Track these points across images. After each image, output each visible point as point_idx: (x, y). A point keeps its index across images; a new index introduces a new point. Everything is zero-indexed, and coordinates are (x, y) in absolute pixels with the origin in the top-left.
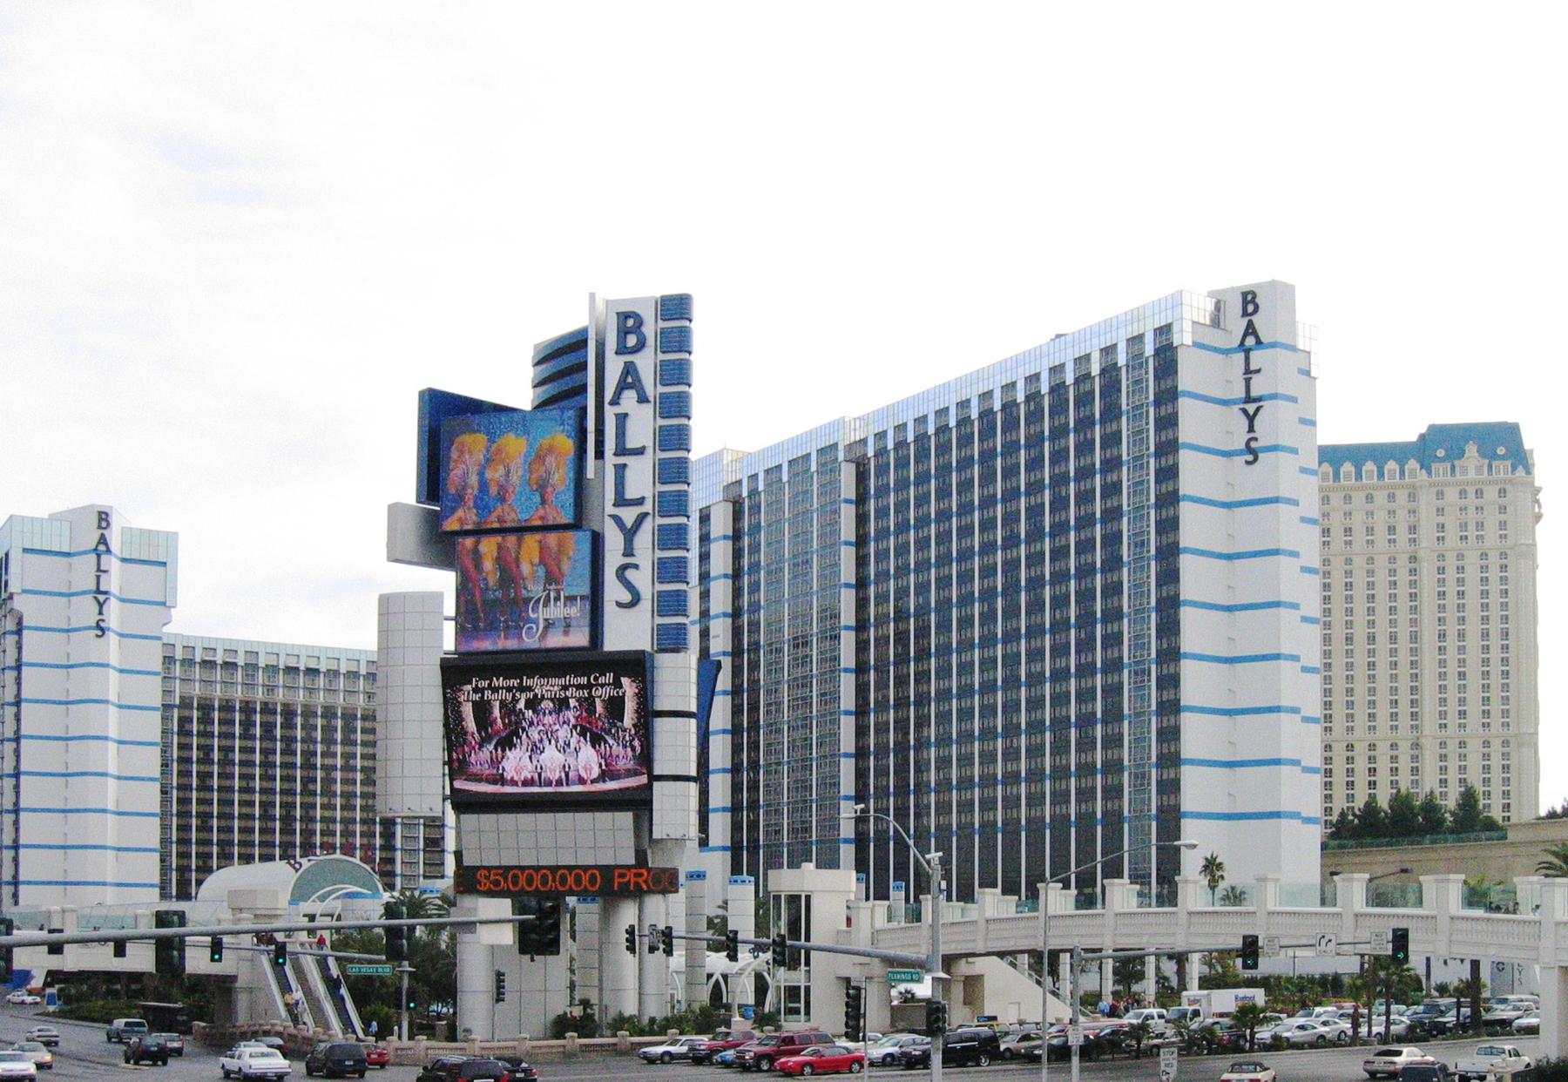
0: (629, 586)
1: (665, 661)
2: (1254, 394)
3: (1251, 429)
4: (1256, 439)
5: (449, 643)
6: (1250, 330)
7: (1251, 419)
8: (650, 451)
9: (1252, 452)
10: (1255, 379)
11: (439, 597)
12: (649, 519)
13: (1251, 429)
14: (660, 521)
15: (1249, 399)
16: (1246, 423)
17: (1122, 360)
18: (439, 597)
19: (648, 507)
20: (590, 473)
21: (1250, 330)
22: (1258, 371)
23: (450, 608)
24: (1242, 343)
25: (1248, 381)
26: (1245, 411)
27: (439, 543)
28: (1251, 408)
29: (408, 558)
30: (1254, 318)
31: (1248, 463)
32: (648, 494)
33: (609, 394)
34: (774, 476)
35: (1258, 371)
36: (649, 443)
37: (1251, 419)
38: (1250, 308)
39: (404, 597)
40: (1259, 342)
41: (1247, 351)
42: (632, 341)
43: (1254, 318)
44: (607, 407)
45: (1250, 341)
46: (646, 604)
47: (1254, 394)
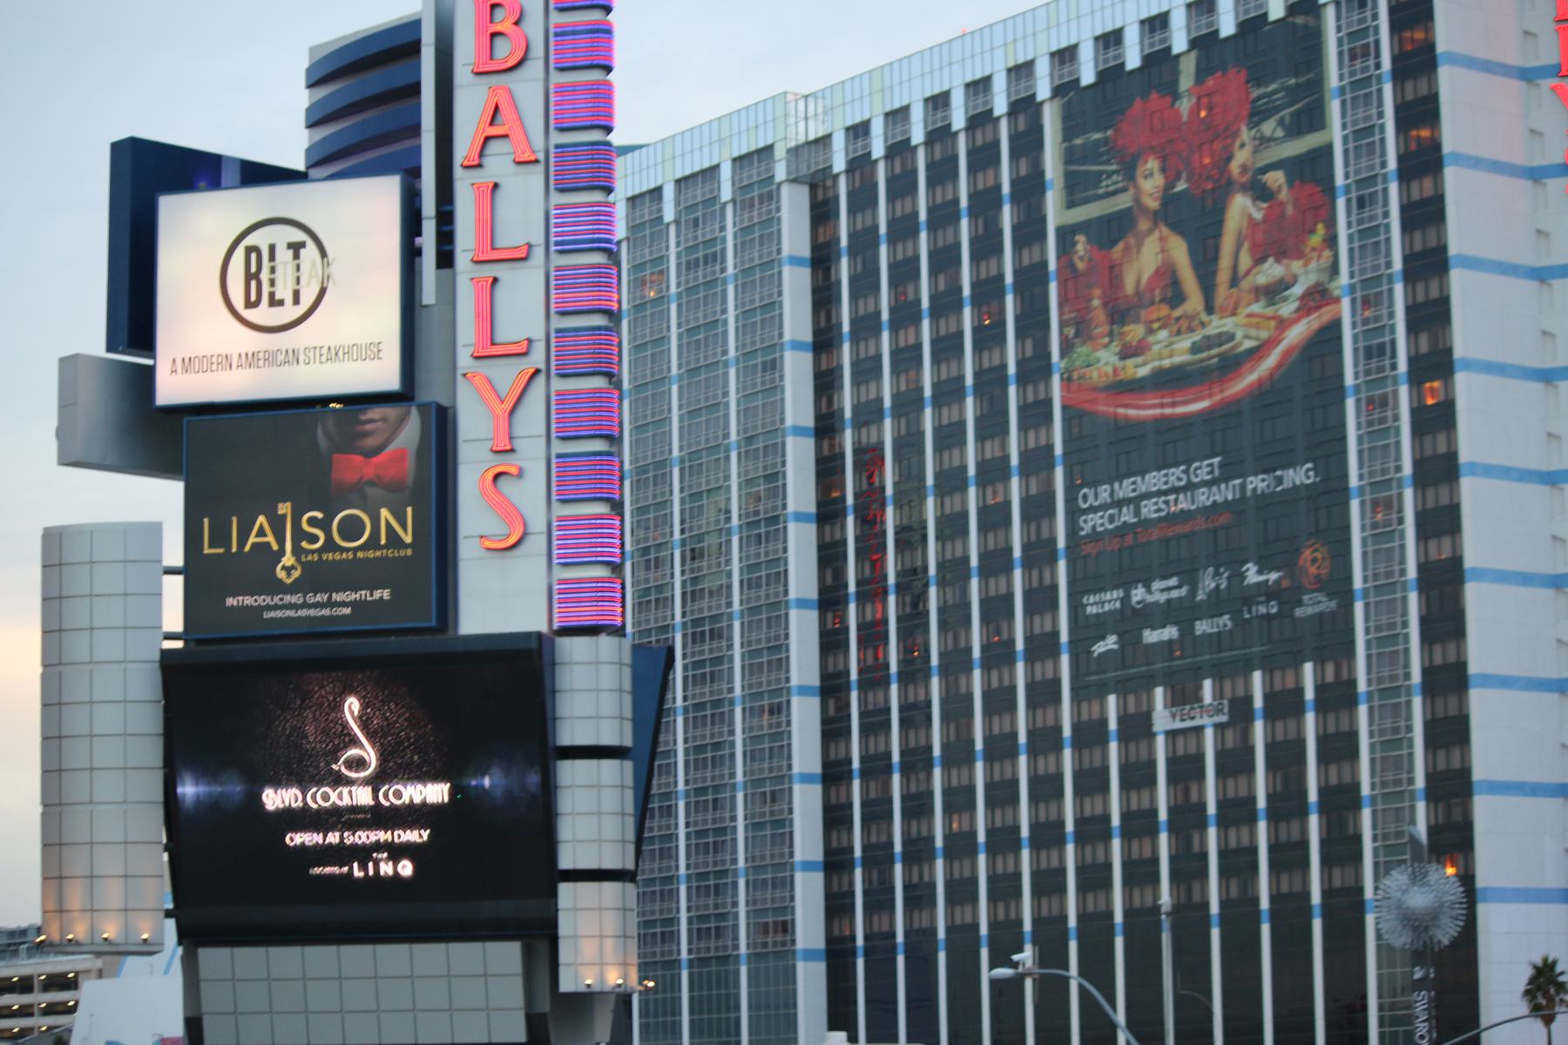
0: (508, 511)
1: (573, 649)
5: (173, 619)
8: (539, 253)
11: (153, 531)
12: (541, 379)
14: (558, 385)
18: (153, 531)
19: (537, 358)
20: (428, 295)
23: (174, 554)
27: (148, 430)
29: (109, 462)
32: (538, 333)
33: (463, 146)
36: (538, 237)
39: (88, 533)
42: (503, 49)
44: (458, 172)
46: (537, 544)
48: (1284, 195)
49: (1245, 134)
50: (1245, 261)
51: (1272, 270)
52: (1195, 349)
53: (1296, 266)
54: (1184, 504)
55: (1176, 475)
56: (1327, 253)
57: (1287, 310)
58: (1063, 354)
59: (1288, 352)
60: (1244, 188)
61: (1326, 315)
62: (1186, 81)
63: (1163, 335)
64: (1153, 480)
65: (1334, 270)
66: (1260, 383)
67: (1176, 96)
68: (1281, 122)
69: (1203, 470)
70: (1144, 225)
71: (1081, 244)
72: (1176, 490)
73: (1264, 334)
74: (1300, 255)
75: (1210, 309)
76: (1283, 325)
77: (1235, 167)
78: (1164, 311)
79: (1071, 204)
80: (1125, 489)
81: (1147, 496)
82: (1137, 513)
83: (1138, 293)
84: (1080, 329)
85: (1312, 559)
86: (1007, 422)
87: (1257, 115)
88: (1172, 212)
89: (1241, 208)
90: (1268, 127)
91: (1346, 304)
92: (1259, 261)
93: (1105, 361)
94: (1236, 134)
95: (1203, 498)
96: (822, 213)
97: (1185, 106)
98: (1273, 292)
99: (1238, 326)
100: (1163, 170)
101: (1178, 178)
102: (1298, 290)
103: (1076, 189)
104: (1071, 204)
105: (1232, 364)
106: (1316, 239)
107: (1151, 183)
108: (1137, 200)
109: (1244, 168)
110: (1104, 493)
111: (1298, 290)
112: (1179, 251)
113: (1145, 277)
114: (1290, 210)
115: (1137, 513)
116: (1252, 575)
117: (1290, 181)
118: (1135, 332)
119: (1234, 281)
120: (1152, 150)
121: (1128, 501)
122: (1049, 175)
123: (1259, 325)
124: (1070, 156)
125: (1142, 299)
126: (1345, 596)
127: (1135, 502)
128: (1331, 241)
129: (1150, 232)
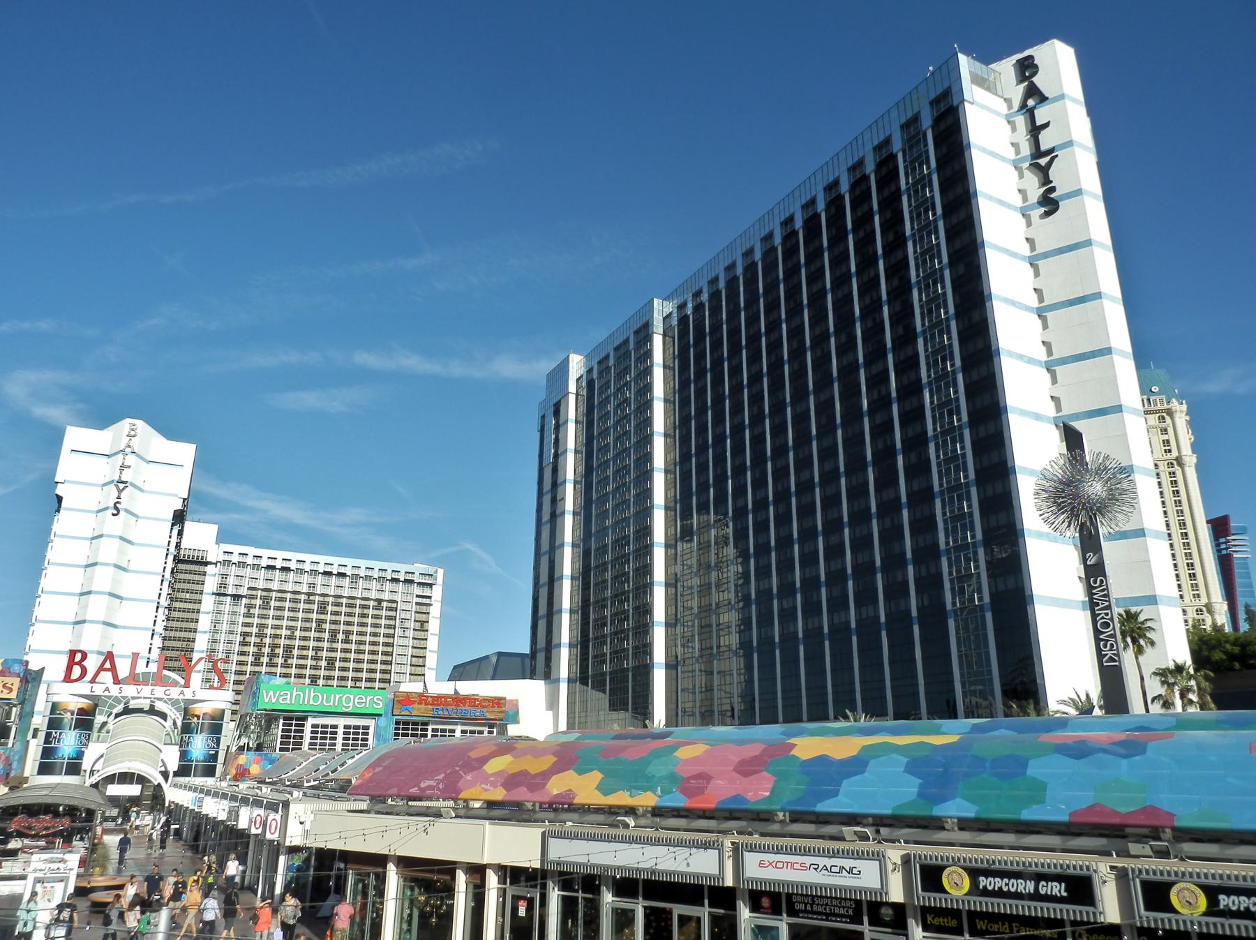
2: (1044, 147)
3: (1046, 180)
4: (1053, 189)
7: (1044, 173)
9: (1049, 204)
13: (1046, 180)
15: (1038, 153)
17: (897, 146)
21: (1033, 91)
22: (1046, 125)
24: (1023, 106)
26: (1036, 167)
28: (1043, 161)
30: (1035, 79)
31: (1047, 214)
34: (622, 351)
35: (1046, 125)
37: (1044, 173)
40: (1043, 99)
41: (1031, 113)
43: (1035, 79)
47: (1044, 147)
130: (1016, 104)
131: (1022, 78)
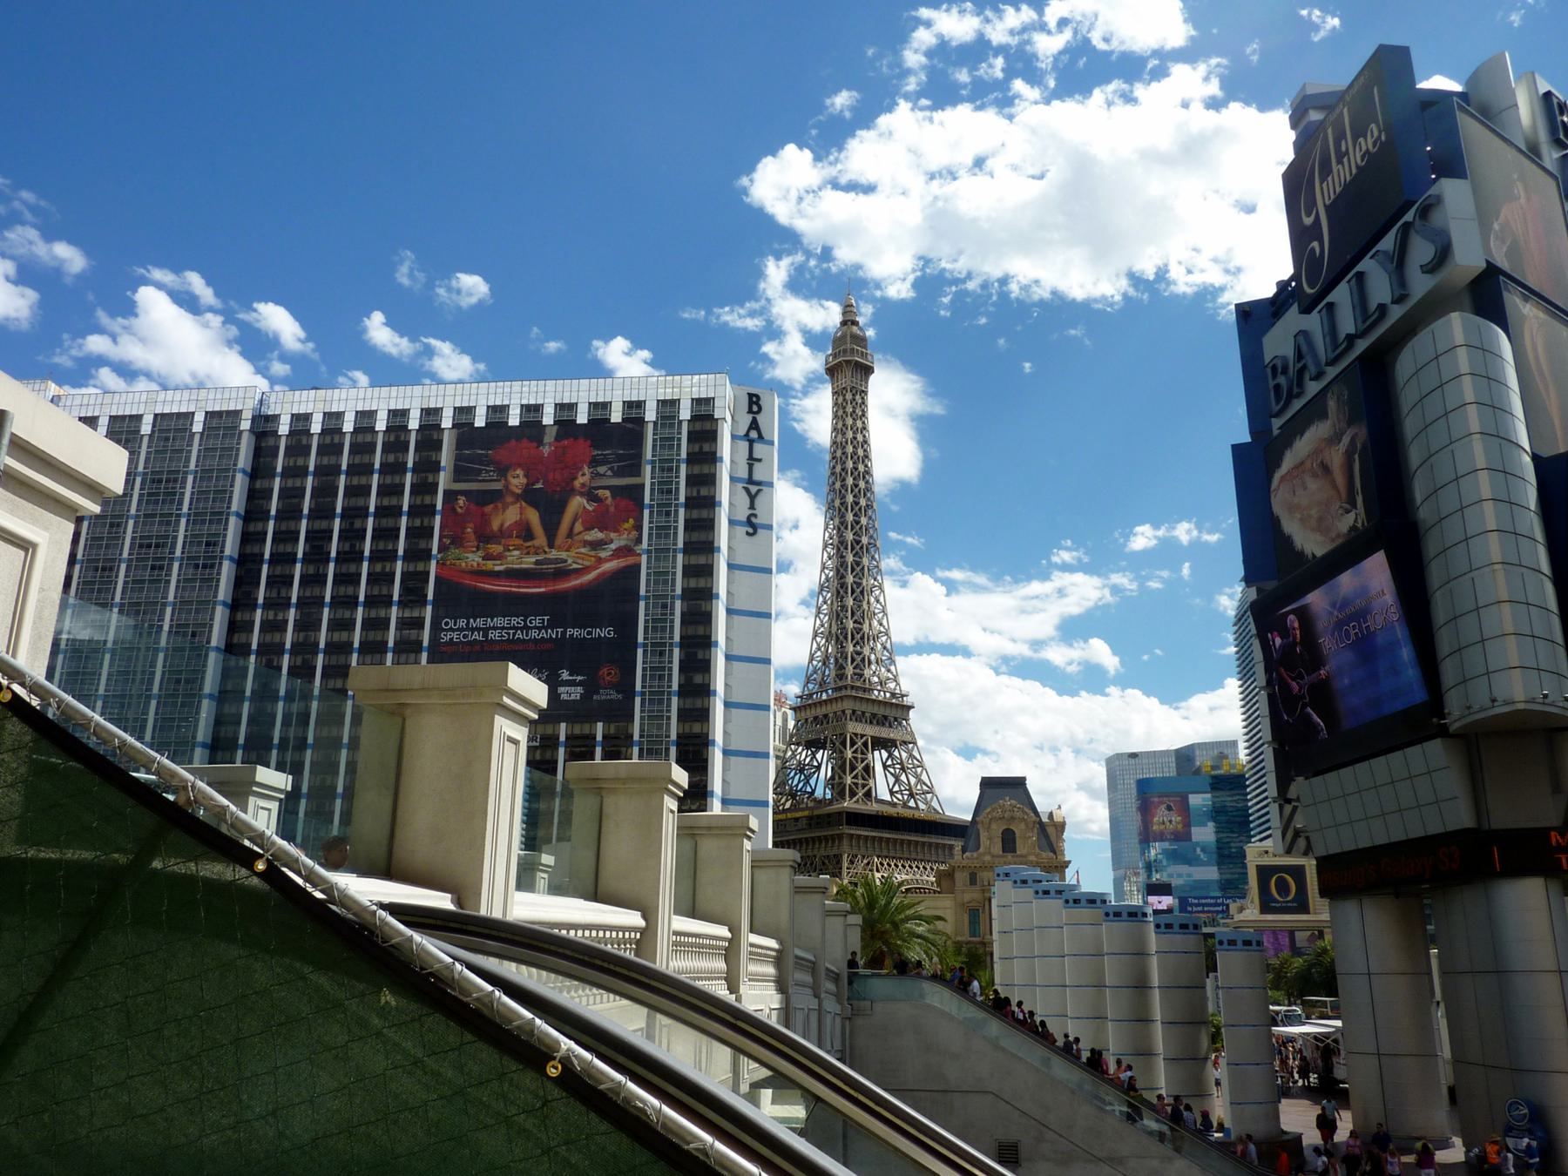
3: (752, 507)
6: (754, 425)
7: (752, 498)
10: (757, 466)
13: (752, 507)
15: (751, 481)
16: (748, 501)
21: (754, 425)
24: (747, 435)
25: (751, 467)
26: (747, 490)
28: (753, 489)
37: (752, 498)
38: (755, 408)
40: (760, 437)
45: (754, 434)
47: (756, 477)
48: (609, 501)
49: (586, 470)
50: (578, 527)
51: (595, 535)
52: (537, 563)
53: (613, 535)
54: (519, 635)
55: (515, 621)
56: (634, 534)
57: (603, 554)
58: (440, 551)
59: (603, 574)
60: (582, 494)
61: (630, 560)
62: (549, 437)
63: (517, 553)
64: (498, 621)
65: (639, 540)
66: (581, 585)
67: (540, 442)
68: (611, 469)
69: (537, 622)
70: (509, 499)
71: (461, 501)
72: (516, 629)
73: (587, 563)
74: (617, 531)
75: (551, 546)
76: (600, 561)
77: (577, 484)
78: (519, 542)
79: (456, 480)
80: (480, 622)
81: (495, 628)
82: (485, 635)
83: (500, 530)
84: (454, 539)
85: (608, 673)
86: (402, 582)
87: (594, 462)
88: (529, 496)
89: (577, 503)
90: (602, 469)
91: (644, 558)
92: (588, 529)
93: (474, 559)
94: (581, 468)
95: (534, 634)
96: (258, 452)
97: (546, 450)
98: (597, 545)
99: (571, 558)
100: (526, 476)
101: (537, 481)
102: (613, 546)
103: (459, 473)
104: (456, 480)
105: (563, 573)
106: (626, 526)
107: (517, 480)
108: (507, 487)
109: (583, 485)
110: (462, 623)
111: (613, 546)
112: (533, 517)
113: (507, 524)
114: (612, 509)
115: (485, 635)
116: (565, 675)
117: (613, 497)
118: (496, 548)
119: (570, 534)
120: (519, 465)
121: (478, 629)
122: (443, 464)
123: (586, 558)
124: (459, 458)
125: (502, 534)
126: (629, 693)
127: (486, 631)
128: (639, 528)
129: (513, 503)
130: (742, 432)
131: (750, 411)
